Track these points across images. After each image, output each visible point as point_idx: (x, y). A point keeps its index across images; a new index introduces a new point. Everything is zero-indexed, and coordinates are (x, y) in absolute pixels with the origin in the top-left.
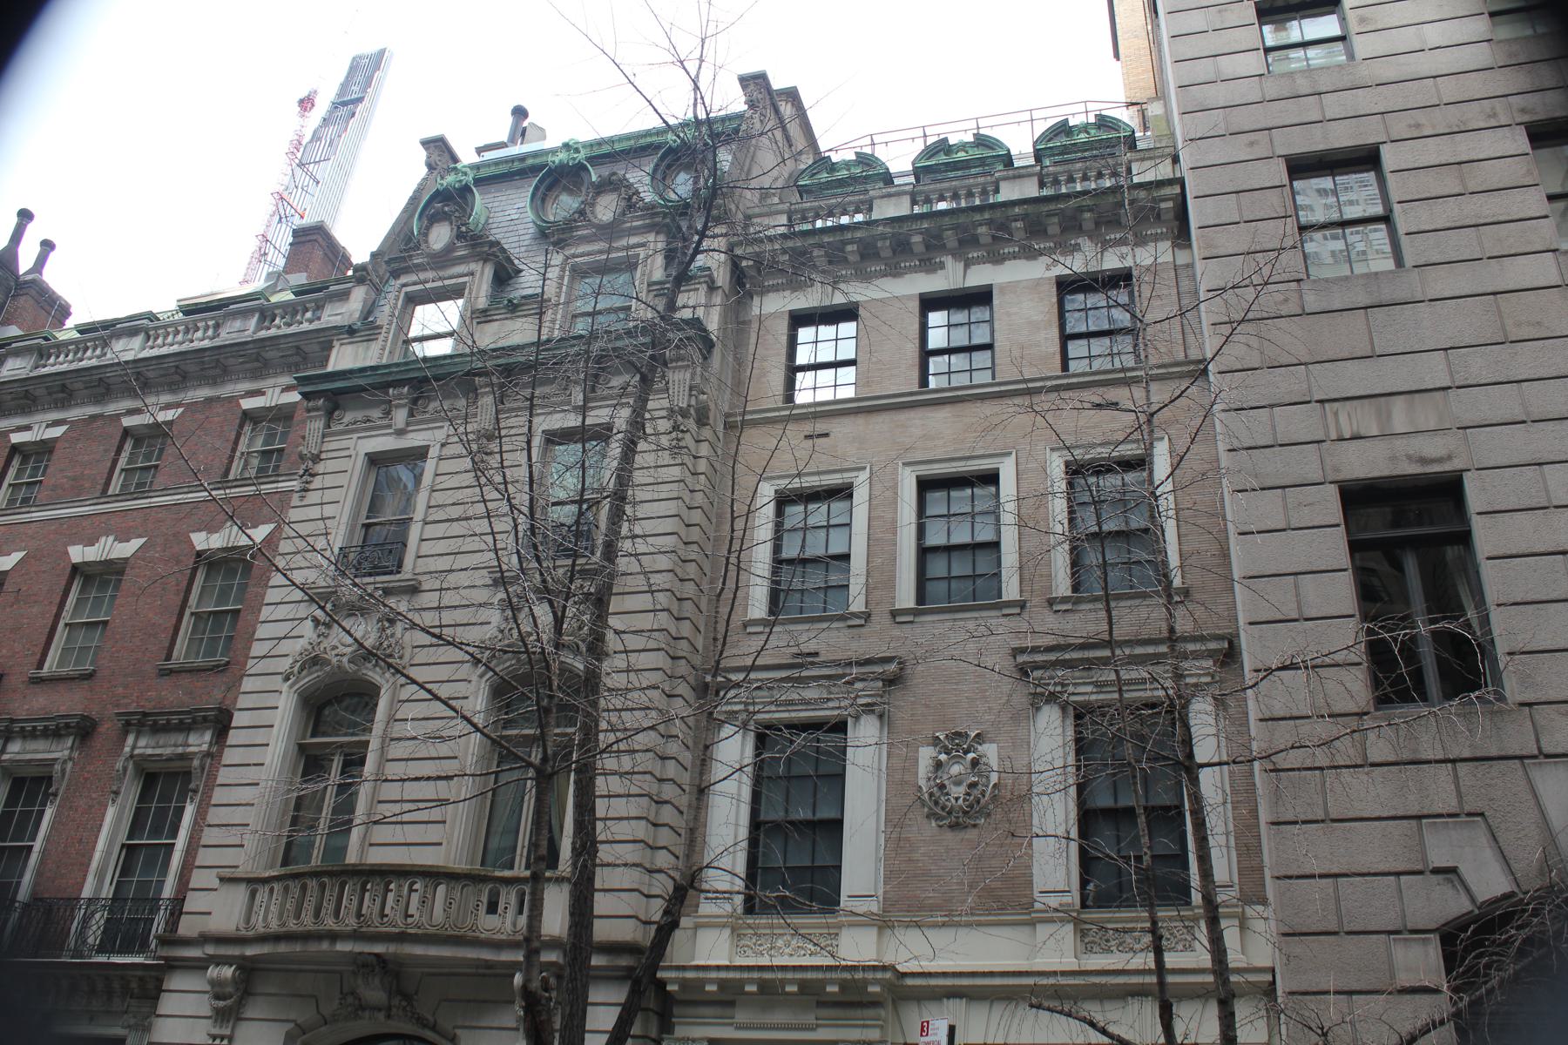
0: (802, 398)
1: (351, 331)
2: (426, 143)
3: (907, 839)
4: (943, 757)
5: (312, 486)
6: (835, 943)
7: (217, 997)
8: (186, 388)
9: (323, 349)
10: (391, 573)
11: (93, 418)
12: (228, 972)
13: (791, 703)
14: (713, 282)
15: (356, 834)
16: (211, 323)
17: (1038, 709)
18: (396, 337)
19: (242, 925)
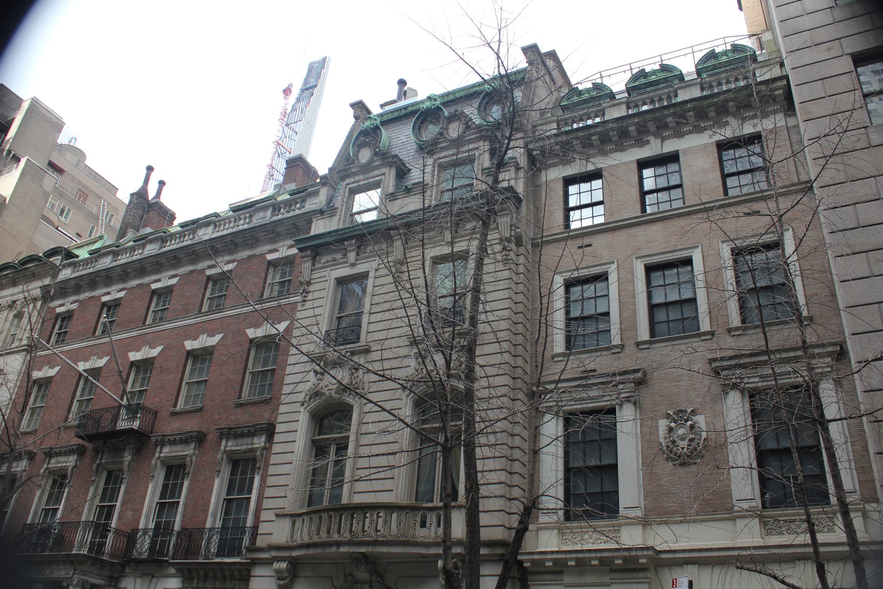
0: (574, 226)
1: (321, 212)
2: (353, 105)
3: (656, 474)
4: (673, 425)
5: (308, 299)
6: (618, 535)
7: (279, 579)
8: (237, 252)
9: (307, 224)
10: (354, 343)
11: (191, 272)
12: (284, 565)
13: (582, 399)
14: (518, 165)
15: (346, 488)
16: (247, 215)
17: (727, 393)
18: (346, 213)
19: (289, 540)
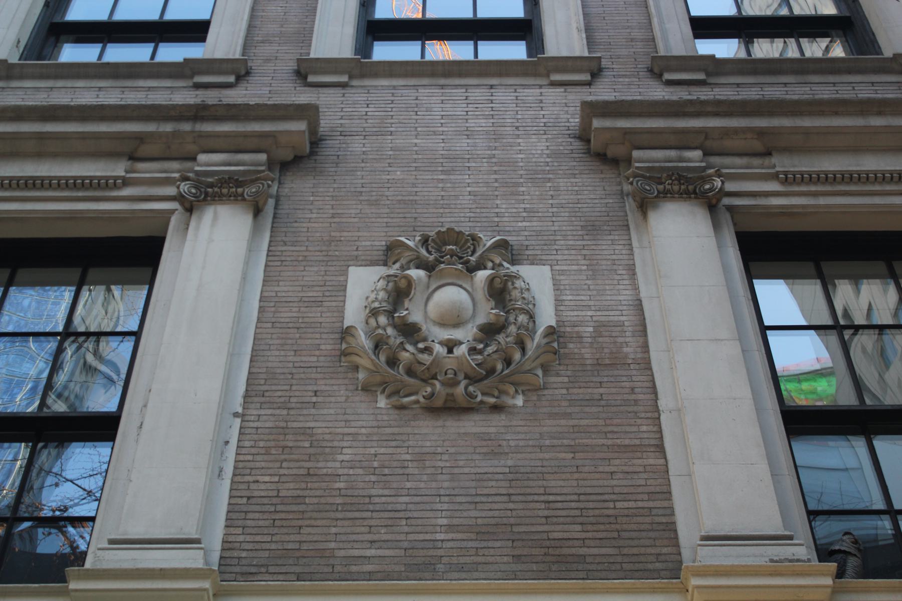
3: (306, 432)
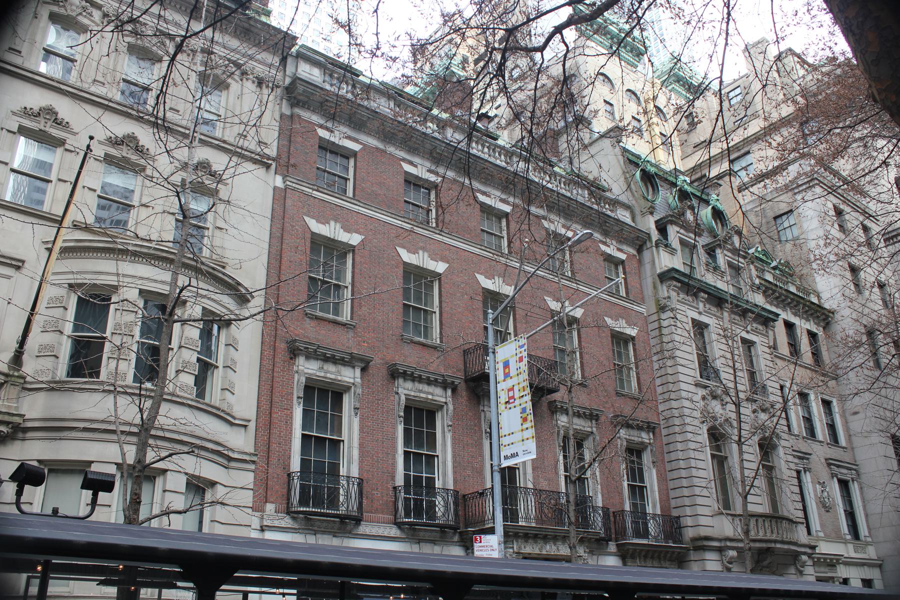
17: (833, 477)
